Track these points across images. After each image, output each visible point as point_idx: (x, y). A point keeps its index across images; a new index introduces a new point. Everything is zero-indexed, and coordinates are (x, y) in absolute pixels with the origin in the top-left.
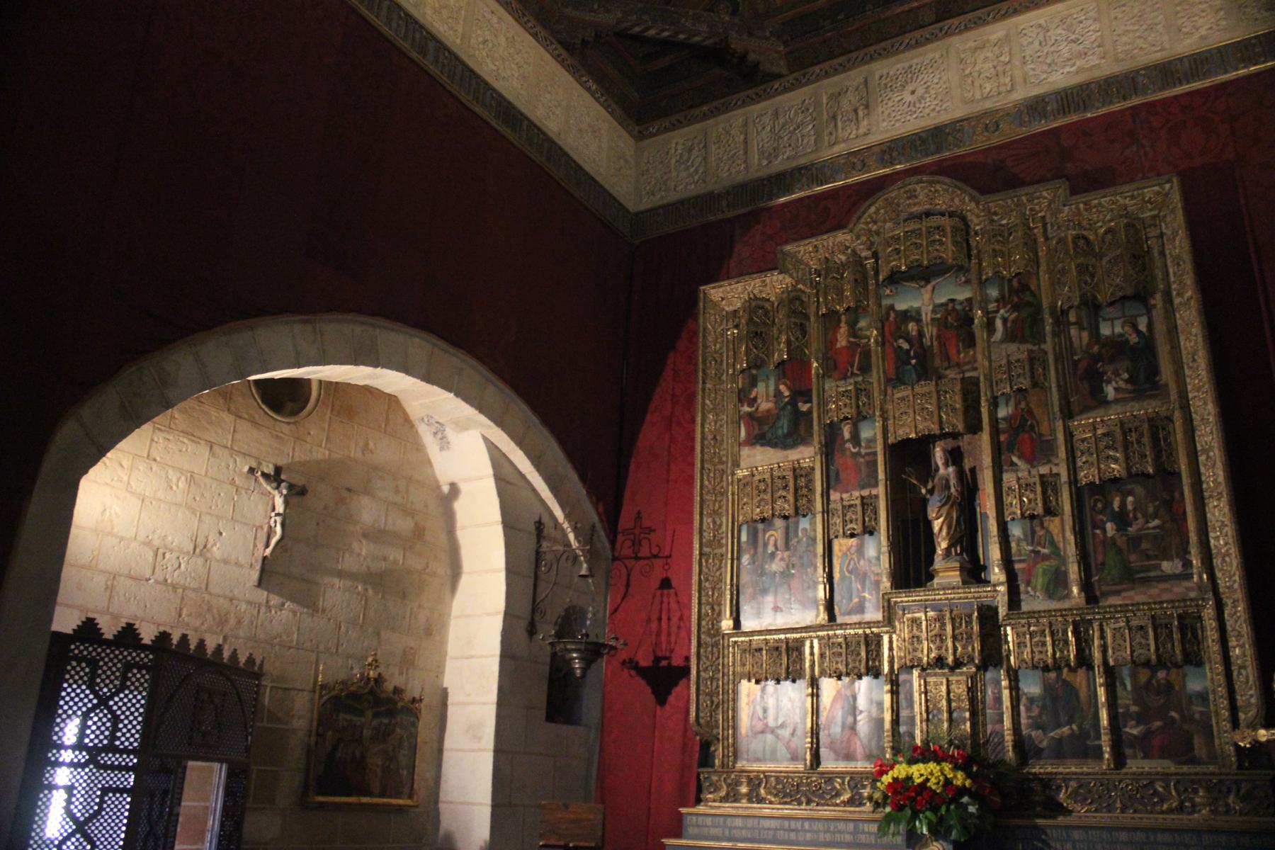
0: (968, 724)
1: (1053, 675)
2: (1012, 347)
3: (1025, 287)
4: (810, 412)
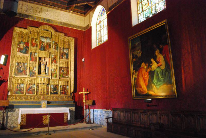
1: (54, 86)
2: (55, 50)
3: (57, 43)
4: (28, 50)
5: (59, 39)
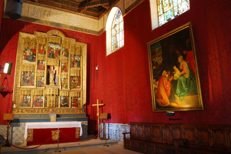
0: (55, 103)
1: (65, 97)
2: (65, 57)
3: (67, 50)
4: (35, 57)
5: (69, 45)
